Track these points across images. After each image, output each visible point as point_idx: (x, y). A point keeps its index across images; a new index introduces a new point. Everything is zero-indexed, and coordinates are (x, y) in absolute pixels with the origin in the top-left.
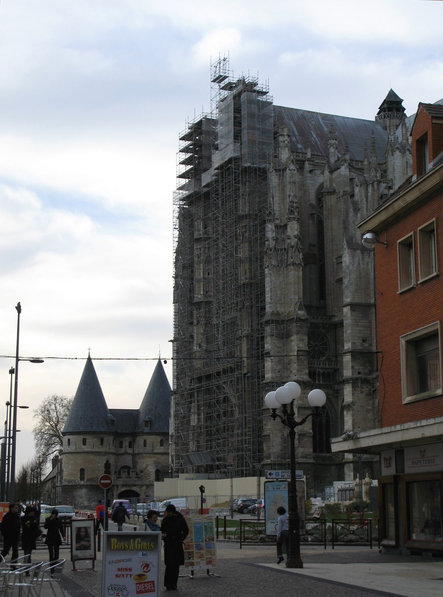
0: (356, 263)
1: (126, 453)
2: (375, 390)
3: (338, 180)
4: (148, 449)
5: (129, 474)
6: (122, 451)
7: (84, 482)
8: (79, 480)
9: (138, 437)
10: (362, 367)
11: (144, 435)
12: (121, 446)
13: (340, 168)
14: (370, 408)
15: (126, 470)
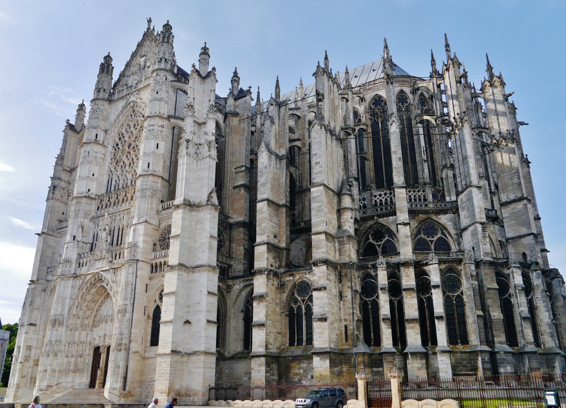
0: (272, 166)
2: (283, 285)
3: (243, 106)
10: (273, 261)
13: (246, 96)
14: (278, 301)
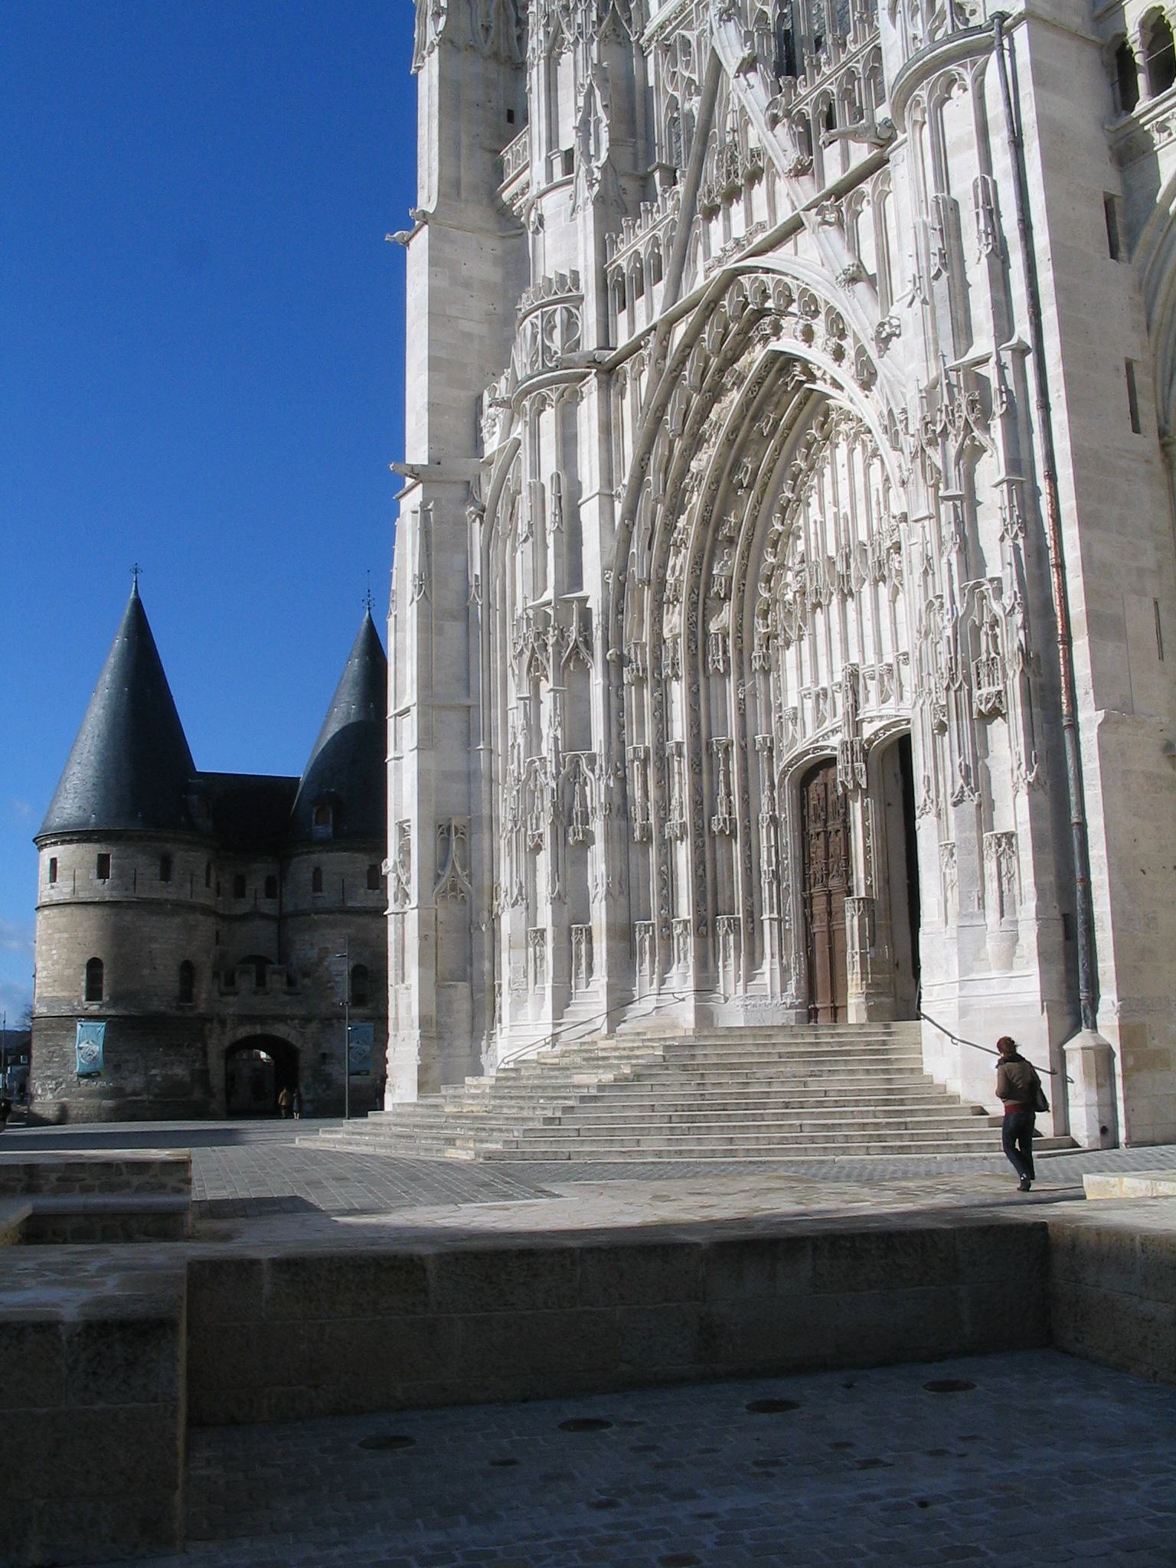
1: (254, 915)
4: (329, 896)
5: (261, 980)
6: (243, 907)
7: (101, 1006)
8: (84, 998)
9: (296, 859)
11: (313, 853)
12: (240, 892)
15: (253, 967)
